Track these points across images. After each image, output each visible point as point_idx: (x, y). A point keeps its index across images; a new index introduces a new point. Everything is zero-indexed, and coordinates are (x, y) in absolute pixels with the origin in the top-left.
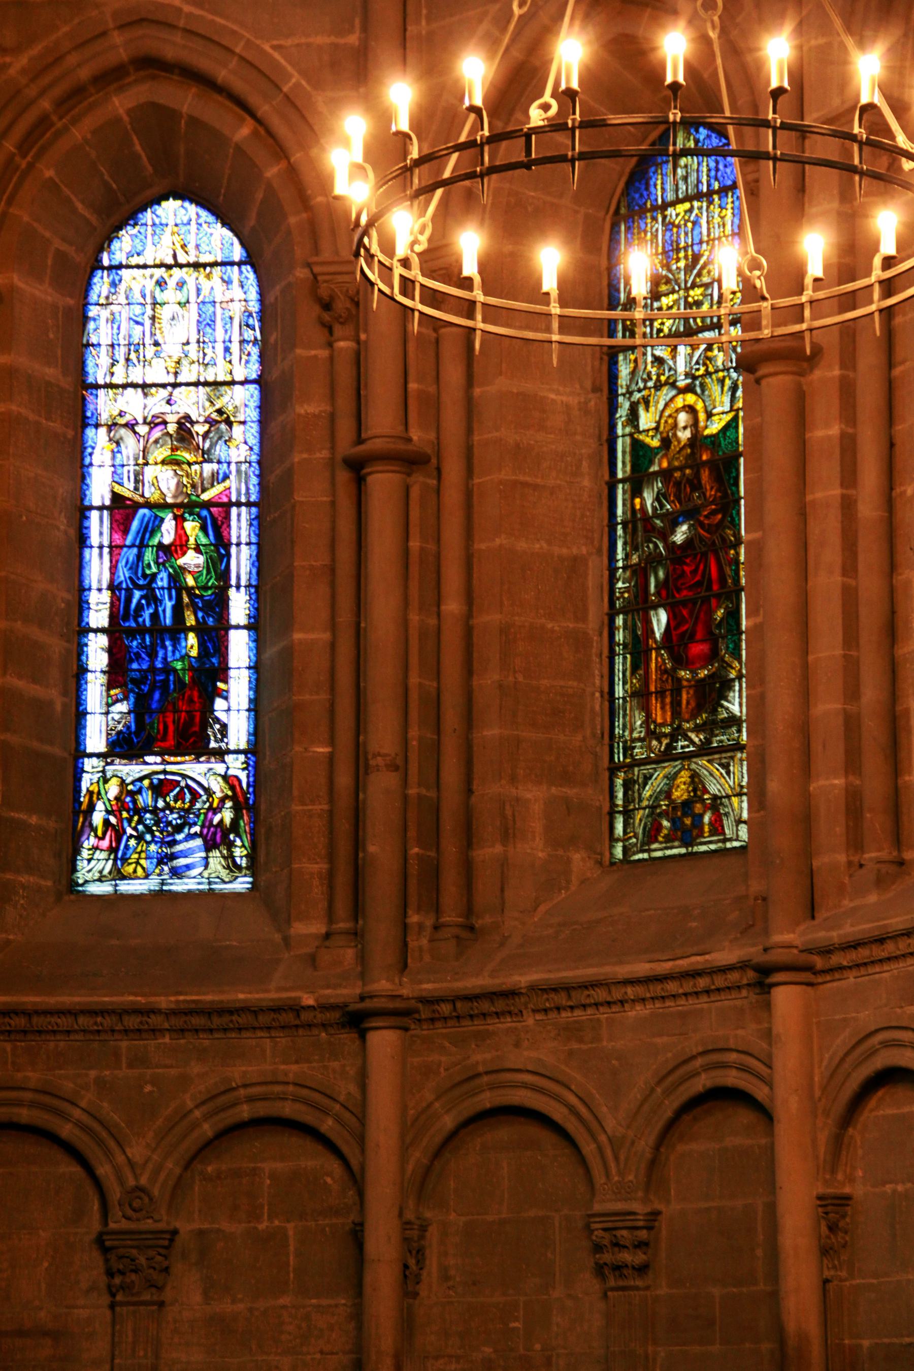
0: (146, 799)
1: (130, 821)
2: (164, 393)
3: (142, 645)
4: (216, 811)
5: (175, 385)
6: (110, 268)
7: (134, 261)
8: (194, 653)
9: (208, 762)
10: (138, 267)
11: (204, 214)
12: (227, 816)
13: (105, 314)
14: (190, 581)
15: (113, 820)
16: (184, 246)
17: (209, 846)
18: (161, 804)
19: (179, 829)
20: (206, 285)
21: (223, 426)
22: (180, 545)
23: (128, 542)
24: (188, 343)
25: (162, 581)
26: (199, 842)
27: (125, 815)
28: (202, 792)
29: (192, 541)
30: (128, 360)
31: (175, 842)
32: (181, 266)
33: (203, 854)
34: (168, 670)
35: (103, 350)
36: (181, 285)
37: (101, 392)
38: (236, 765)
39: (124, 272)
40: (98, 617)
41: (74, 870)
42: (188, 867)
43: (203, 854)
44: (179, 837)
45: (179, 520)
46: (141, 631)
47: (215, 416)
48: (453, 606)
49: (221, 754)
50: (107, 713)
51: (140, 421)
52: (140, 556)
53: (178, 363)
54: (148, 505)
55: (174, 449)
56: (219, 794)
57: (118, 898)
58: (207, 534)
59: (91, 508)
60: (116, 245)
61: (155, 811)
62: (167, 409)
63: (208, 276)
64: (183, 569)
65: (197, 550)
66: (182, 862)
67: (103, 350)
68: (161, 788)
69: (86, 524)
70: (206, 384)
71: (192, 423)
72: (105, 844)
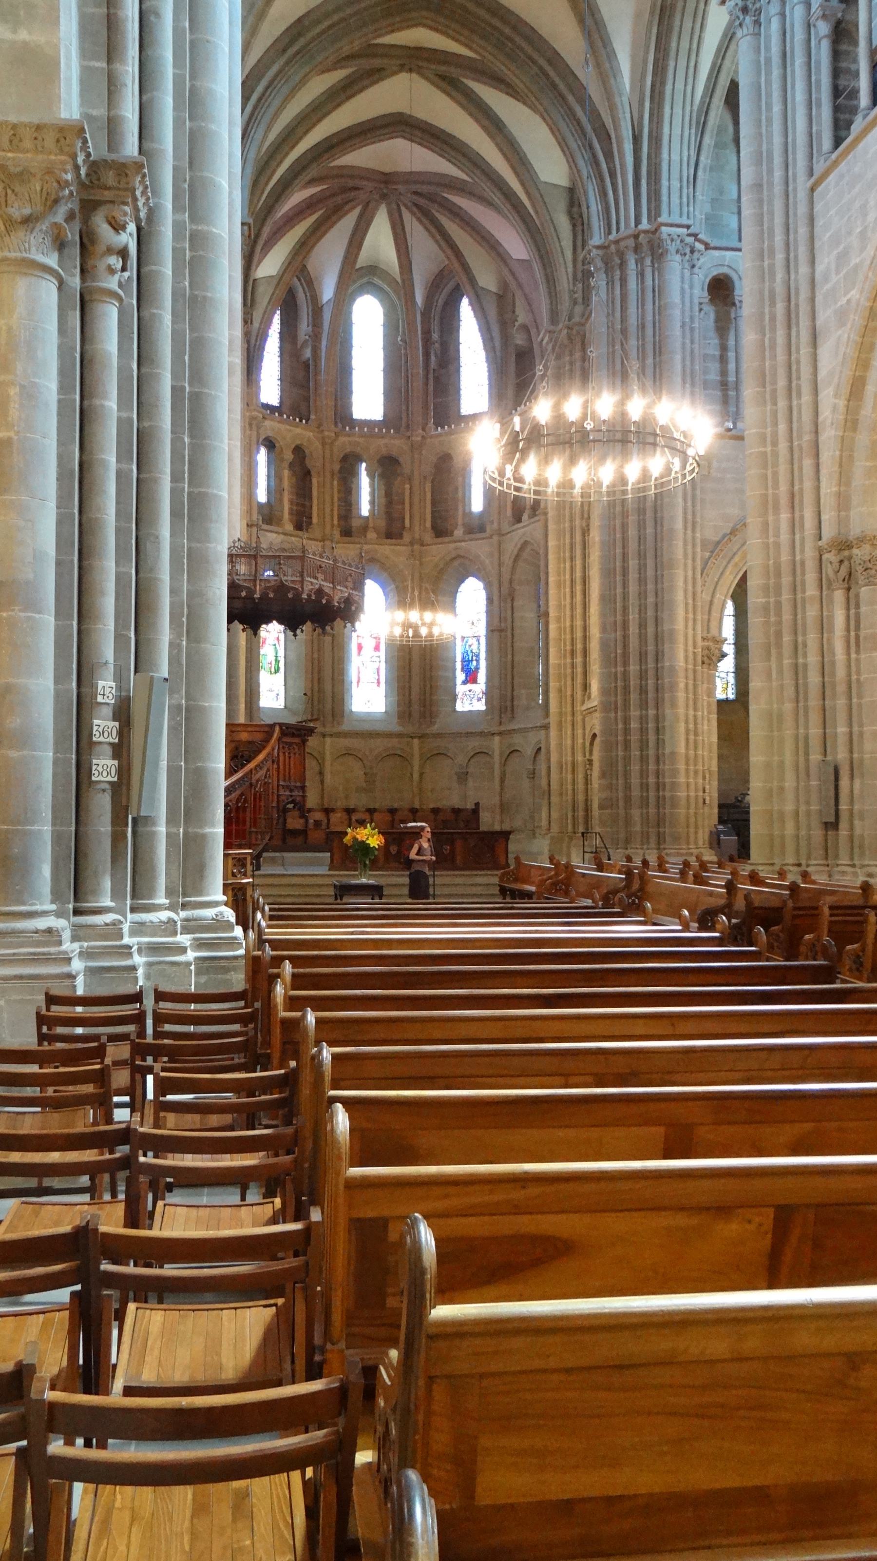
48: (510, 657)
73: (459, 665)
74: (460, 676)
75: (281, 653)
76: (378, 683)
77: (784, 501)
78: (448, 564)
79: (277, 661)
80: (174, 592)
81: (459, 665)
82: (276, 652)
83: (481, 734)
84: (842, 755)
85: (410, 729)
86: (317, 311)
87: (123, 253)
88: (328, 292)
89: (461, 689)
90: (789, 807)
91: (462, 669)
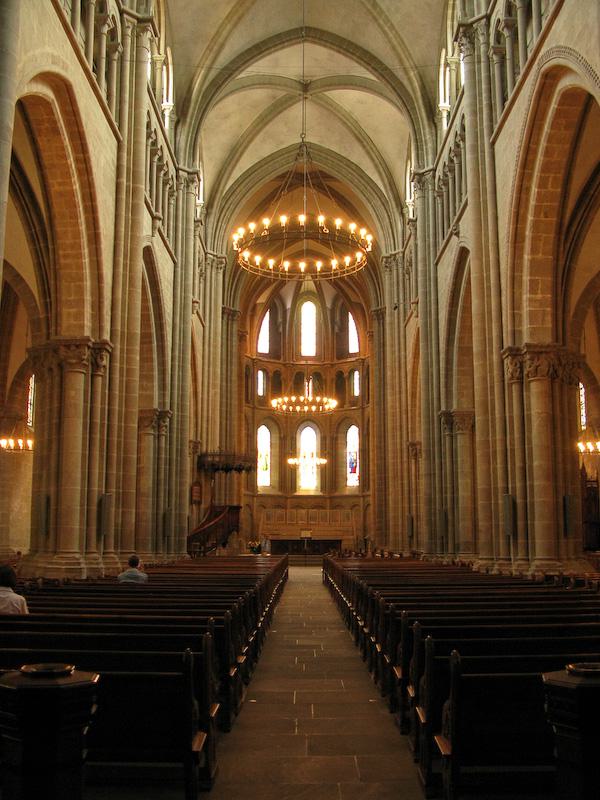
74: (349, 470)
77: (398, 428)
78: (342, 421)
80: (176, 489)
83: (356, 496)
84: (414, 513)
85: (327, 495)
86: (285, 311)
87: (166, 426)
88: (289, 305)
89: (349, 476)
90: (400, 531)
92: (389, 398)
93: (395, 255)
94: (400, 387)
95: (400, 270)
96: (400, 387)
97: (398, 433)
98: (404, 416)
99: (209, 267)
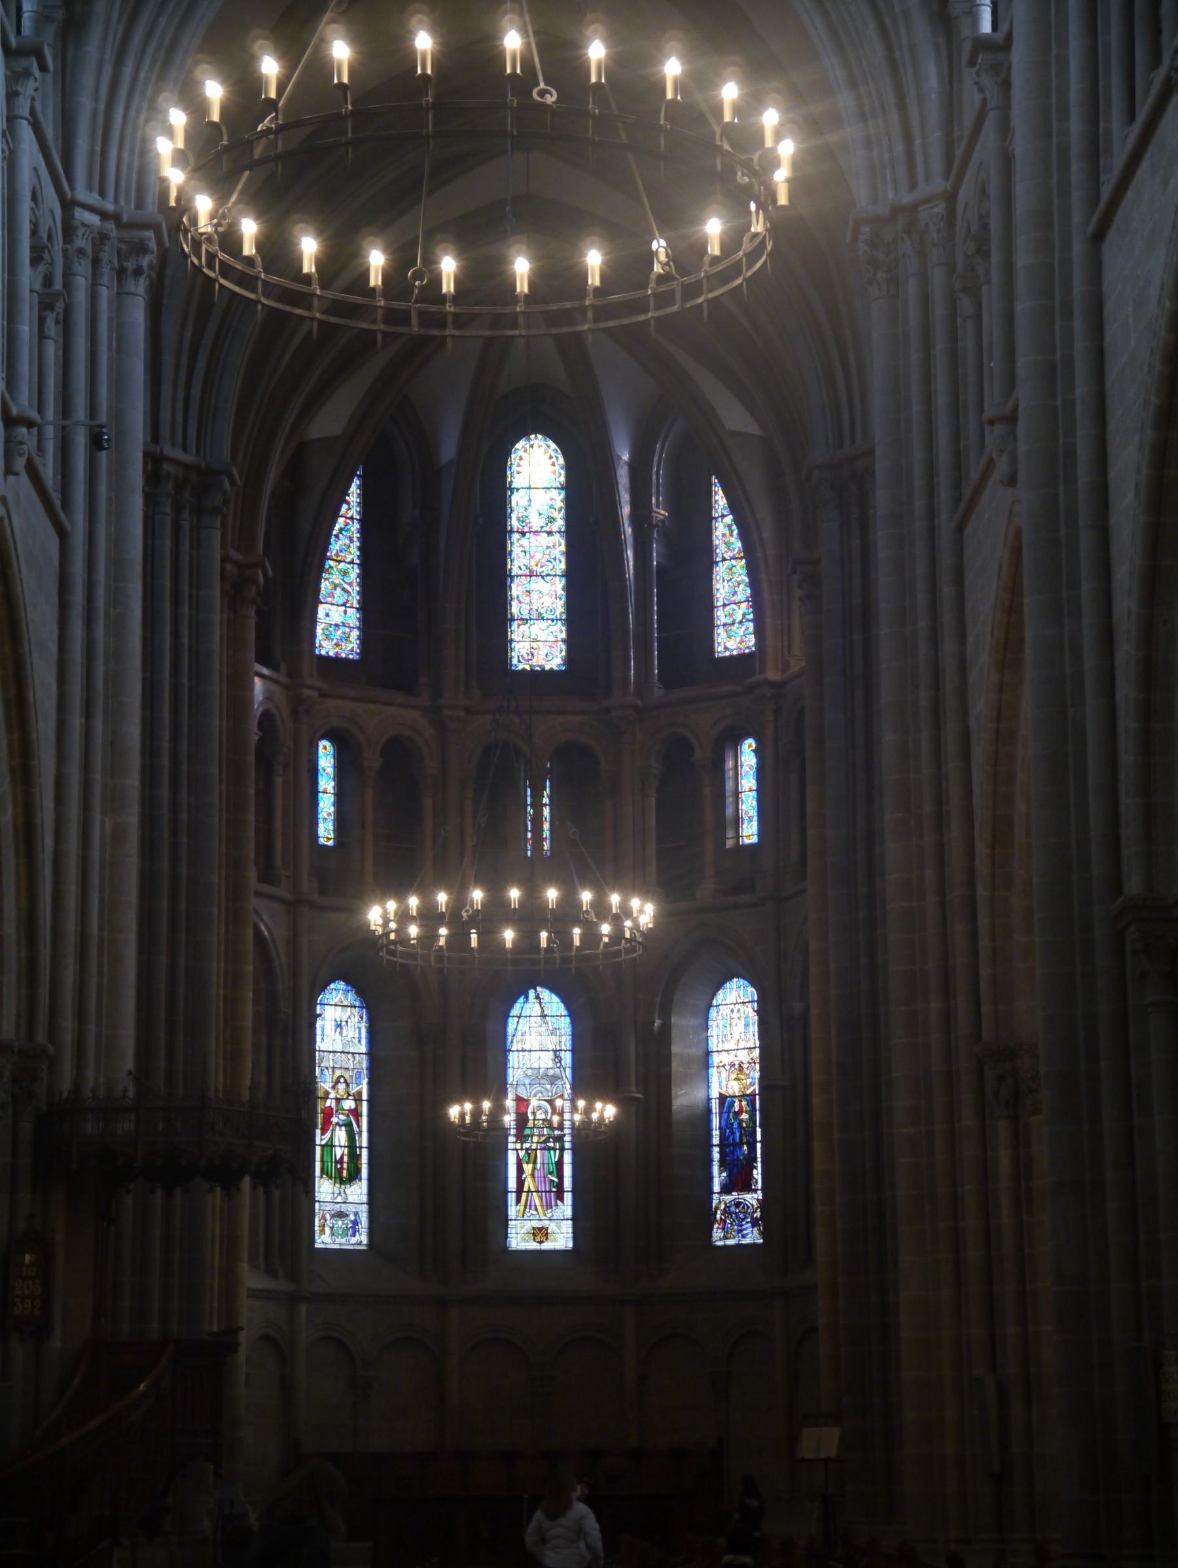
0: (733, 1209)
1: (728, 1217)
2: (734, 1053)
3: (730, 1150)
4: (754, 1212)
5: (738, 1050)
6: (716, 1006)
7: (724, 1002)
8: (746, 1153)
9: (752, 1193)
10: (725, 1005)
11: (746, 982)
12: (758, 1214)
13: (715, 1024)
14: (744, 1125)
15: (723, 1217)
16: (739, 996)
17: (753, 1226)
18: (737, 1211)
19: (743, 1220)
20: (747, 1010)
21: (753, 1064)
22: (741, 1111)
23: (724, 1111)
24: (741, 1033)
25: (735, 1126)
26: (749, 1225)
27: (727, 1215)
28: (750, 1206)
29: (744, 1109)
30: (723, 1041)
31: (742, 1225)
32: (738, 1003)
33: (751, 1229)
34: (738, 1159)
35: (715, 1037)
36: (739, 1011)
37: (714, 1054)
38: (759, 1195)
39: (721, 1007)
40: (716, 1141)
41: (711, 1236)
42: (747, 1234)
43: (751, 1229)
44: (744, 1223)
45: (740, 1101)
46: (730, 1145)
47: (750, 1061)
49: (755, 1191)
50: (720, 1177)
51: (727, 1064)
52: (728, 1116)
53: (738, 1041)
54: (730, 1096)
55: (738, 1074)
56: (756, 1206)
57: (725, 1246)
58: (749, 1107)
59: (712, 1099)
60: (718, 997)
61: (736, 1213)
62: (735, 1059)
63: (747, 1007)
64: (742, 1121)
65: (746, 1113)
66: (745, 1232)
67: (715, 1037)
68: (738, 1205)
69: (710, 1105)
70: (747, 1048)
71: (743, 1064)
72: (721, 1226)
73: (716, 1155)
74: (718, 1179)
75: (364, 1141)
76: (560, 1196)
79: (354, 1157)
81: (716, 1155)
82: (351, 1136)
89: (720, 1200)
91: (722, 1162)
92: (893, 850)
93: (913, 208)
94: (940, 799)
95: (938, 276)
96: (940, 799)
97: (935, 1004)
98: (959, 928)
99: (83, 268)
